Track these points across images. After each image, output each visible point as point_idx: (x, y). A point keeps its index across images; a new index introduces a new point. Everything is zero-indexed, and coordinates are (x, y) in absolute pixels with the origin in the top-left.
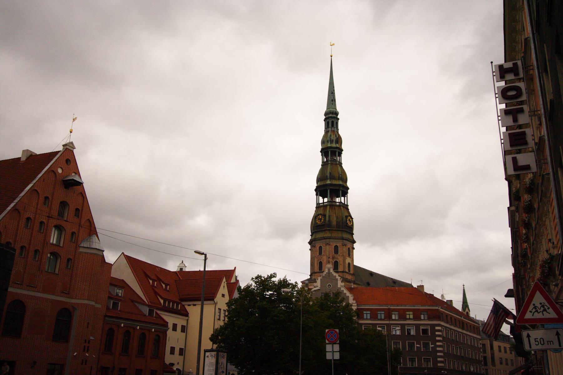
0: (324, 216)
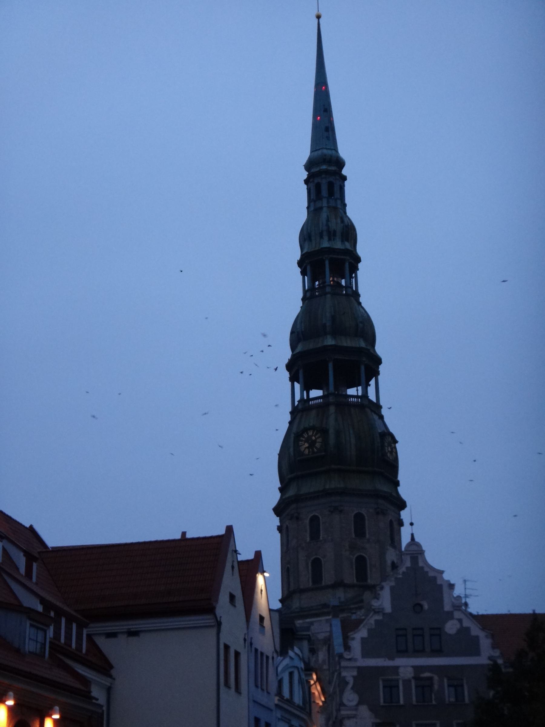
0: (324, 432)
